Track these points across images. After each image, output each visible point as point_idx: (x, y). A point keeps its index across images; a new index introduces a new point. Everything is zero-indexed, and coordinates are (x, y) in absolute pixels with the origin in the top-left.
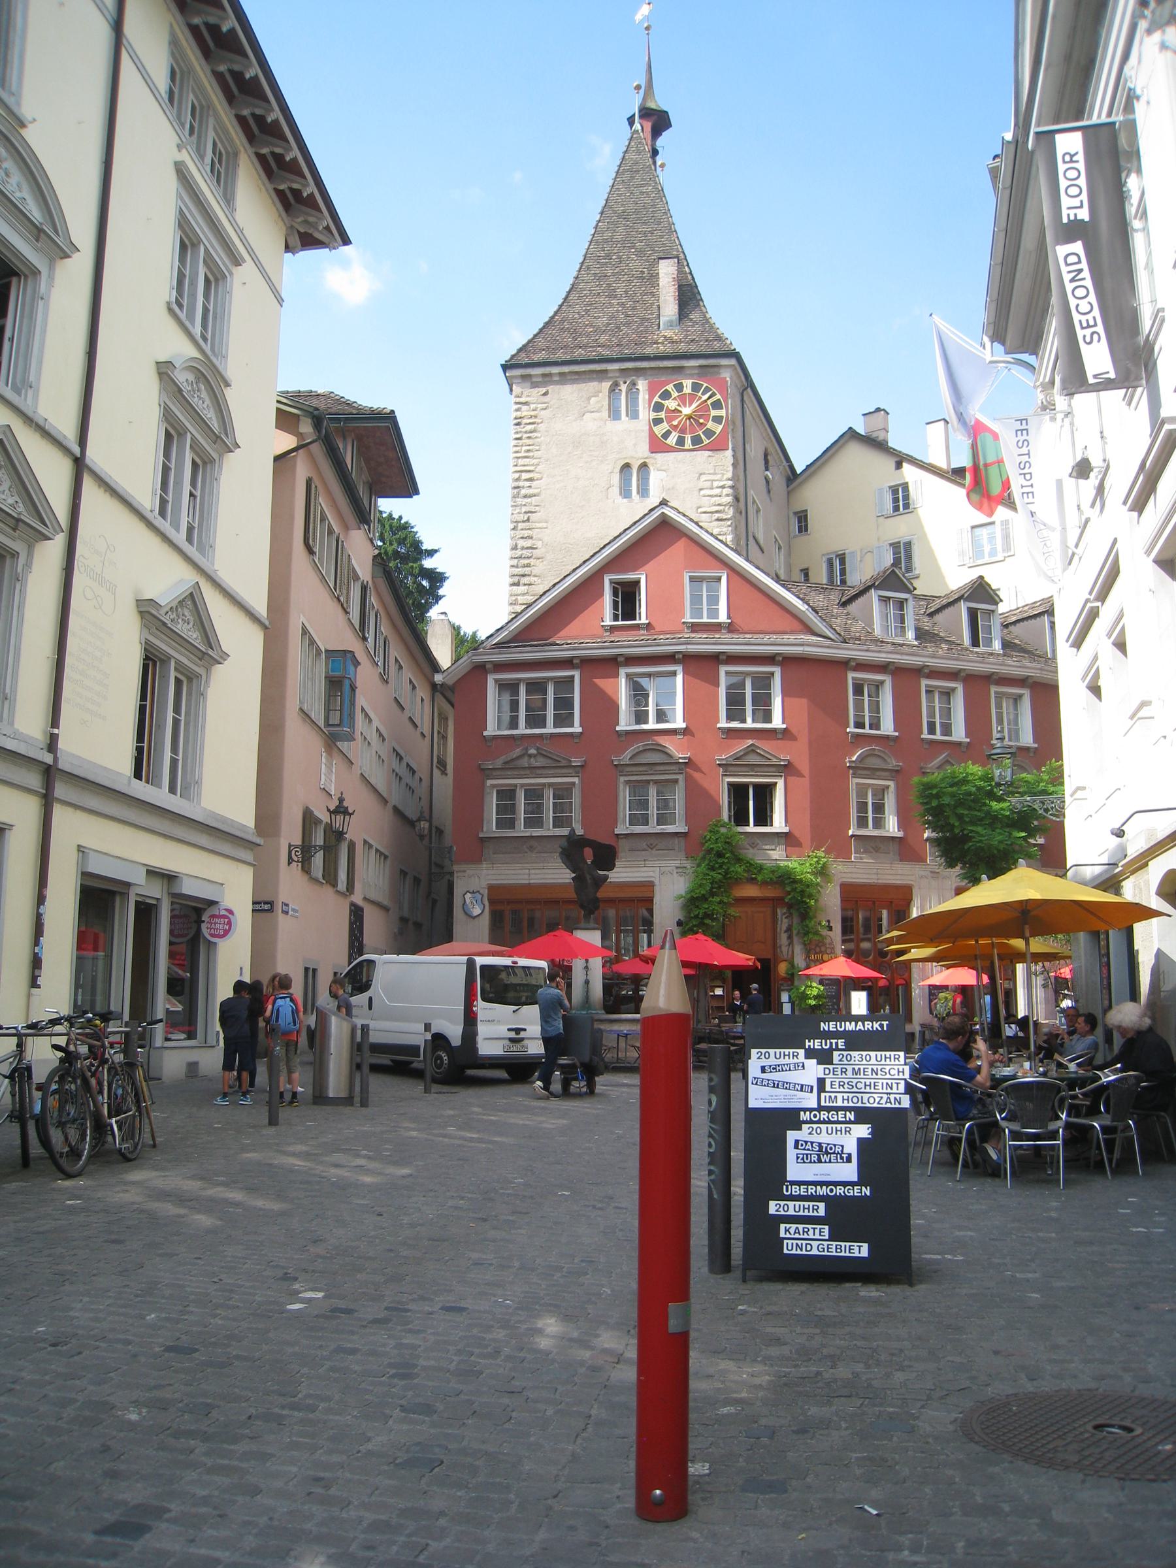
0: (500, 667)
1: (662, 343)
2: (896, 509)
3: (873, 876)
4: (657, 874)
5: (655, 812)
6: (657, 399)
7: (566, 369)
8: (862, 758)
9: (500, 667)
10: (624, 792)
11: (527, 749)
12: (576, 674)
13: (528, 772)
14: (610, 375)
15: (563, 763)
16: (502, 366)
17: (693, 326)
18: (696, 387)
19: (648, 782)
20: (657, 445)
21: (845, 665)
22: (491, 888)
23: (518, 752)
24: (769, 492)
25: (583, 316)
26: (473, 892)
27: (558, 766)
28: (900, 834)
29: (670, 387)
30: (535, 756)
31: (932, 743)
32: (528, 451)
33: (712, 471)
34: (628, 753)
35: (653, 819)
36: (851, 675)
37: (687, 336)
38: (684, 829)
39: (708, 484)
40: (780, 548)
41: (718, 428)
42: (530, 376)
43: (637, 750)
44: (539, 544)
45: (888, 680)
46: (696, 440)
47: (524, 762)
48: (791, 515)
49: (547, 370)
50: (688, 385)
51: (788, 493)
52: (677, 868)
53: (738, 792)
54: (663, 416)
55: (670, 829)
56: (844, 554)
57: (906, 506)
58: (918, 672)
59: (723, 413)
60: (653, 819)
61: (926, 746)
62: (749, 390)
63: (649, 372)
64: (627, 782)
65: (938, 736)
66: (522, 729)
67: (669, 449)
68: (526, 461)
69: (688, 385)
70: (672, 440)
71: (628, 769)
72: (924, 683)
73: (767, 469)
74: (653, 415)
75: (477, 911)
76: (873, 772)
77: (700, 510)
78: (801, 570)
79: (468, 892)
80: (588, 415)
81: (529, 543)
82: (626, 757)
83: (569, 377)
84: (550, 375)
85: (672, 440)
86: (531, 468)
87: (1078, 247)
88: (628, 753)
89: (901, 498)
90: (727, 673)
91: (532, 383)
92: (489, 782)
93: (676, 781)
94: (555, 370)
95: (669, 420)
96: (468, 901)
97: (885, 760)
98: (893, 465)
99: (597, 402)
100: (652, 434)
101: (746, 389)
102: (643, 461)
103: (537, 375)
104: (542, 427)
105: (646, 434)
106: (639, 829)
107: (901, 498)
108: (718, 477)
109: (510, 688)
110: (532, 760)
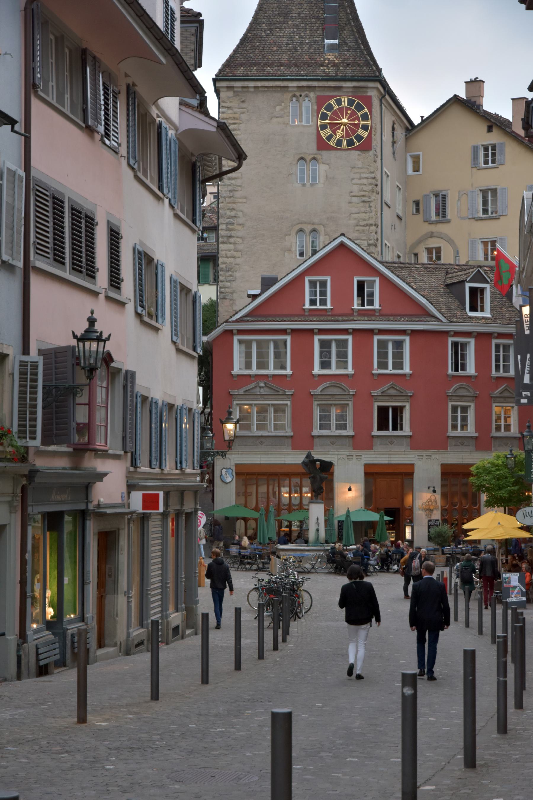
0: (241, 332)
1: (327, 66)
2: (486, 162)
3: (461, 460)
4: (336, 460)
5: (335, 422)
6: (323, 110)
7: (259, 84)
8: (455, 391)
9: (241, 332)
10: (317, 410)
11: (258, 383)
13: (259, 397)
14: (290, 89)
15: (281, 393)
17: (348, 51)
18: (351, 102)
19: (331, 405)
21: (446, 333)
22: (237, 465)
24: (394, 153)
26: (227, 469)
27: (277, 395)
28: (476, 435)
29: (332, 102)
30: (263, 387)
31: (498, 378)
35: (333, 427)
36: (450, 340)
37: (344, 60)
38: (352, 433)
39: (358, 176)
40: (400, 189)
41: (365, 134)
42: (233, 87)
44: (240, 214)
46: (350, 143)
47: (257, 391)
49: (246, 84)
52: (348, 456)
53: (383, 411)
55: (344, 433)
57: (493, 162)
58: (489, 335)
59: (369, 123)
60: (333, 427)
62: (387, 97)
63: (317, 89)
64: (318, 405)
65: (501, 373)
66: (254, 370)
67: (331, 148)
70: (332, 143)
71: (320, 397)
72: (494, 342)
74: (320, 122)
75: (229, 479)
76: (461, 398)
78: (414, 201)
79: (224, 468)
80: (275, 120)
81: (233, 213)
82: (318, 391)
83: (261, 89)
84: (248, 87)
85: (332, 143)
91: (234, 92)
93: (348, 405)
94: (251, 84)
96: (224, 473)
98: (485, 129)
99: (282, 110)
100: (318, 134)
101: (384, 97)
102: (313, 156)
104: (242, 126)
105: (314, 137)
106: (325, 432)
108: (365, 170)
109: (248, 344)
110: (262, 389)
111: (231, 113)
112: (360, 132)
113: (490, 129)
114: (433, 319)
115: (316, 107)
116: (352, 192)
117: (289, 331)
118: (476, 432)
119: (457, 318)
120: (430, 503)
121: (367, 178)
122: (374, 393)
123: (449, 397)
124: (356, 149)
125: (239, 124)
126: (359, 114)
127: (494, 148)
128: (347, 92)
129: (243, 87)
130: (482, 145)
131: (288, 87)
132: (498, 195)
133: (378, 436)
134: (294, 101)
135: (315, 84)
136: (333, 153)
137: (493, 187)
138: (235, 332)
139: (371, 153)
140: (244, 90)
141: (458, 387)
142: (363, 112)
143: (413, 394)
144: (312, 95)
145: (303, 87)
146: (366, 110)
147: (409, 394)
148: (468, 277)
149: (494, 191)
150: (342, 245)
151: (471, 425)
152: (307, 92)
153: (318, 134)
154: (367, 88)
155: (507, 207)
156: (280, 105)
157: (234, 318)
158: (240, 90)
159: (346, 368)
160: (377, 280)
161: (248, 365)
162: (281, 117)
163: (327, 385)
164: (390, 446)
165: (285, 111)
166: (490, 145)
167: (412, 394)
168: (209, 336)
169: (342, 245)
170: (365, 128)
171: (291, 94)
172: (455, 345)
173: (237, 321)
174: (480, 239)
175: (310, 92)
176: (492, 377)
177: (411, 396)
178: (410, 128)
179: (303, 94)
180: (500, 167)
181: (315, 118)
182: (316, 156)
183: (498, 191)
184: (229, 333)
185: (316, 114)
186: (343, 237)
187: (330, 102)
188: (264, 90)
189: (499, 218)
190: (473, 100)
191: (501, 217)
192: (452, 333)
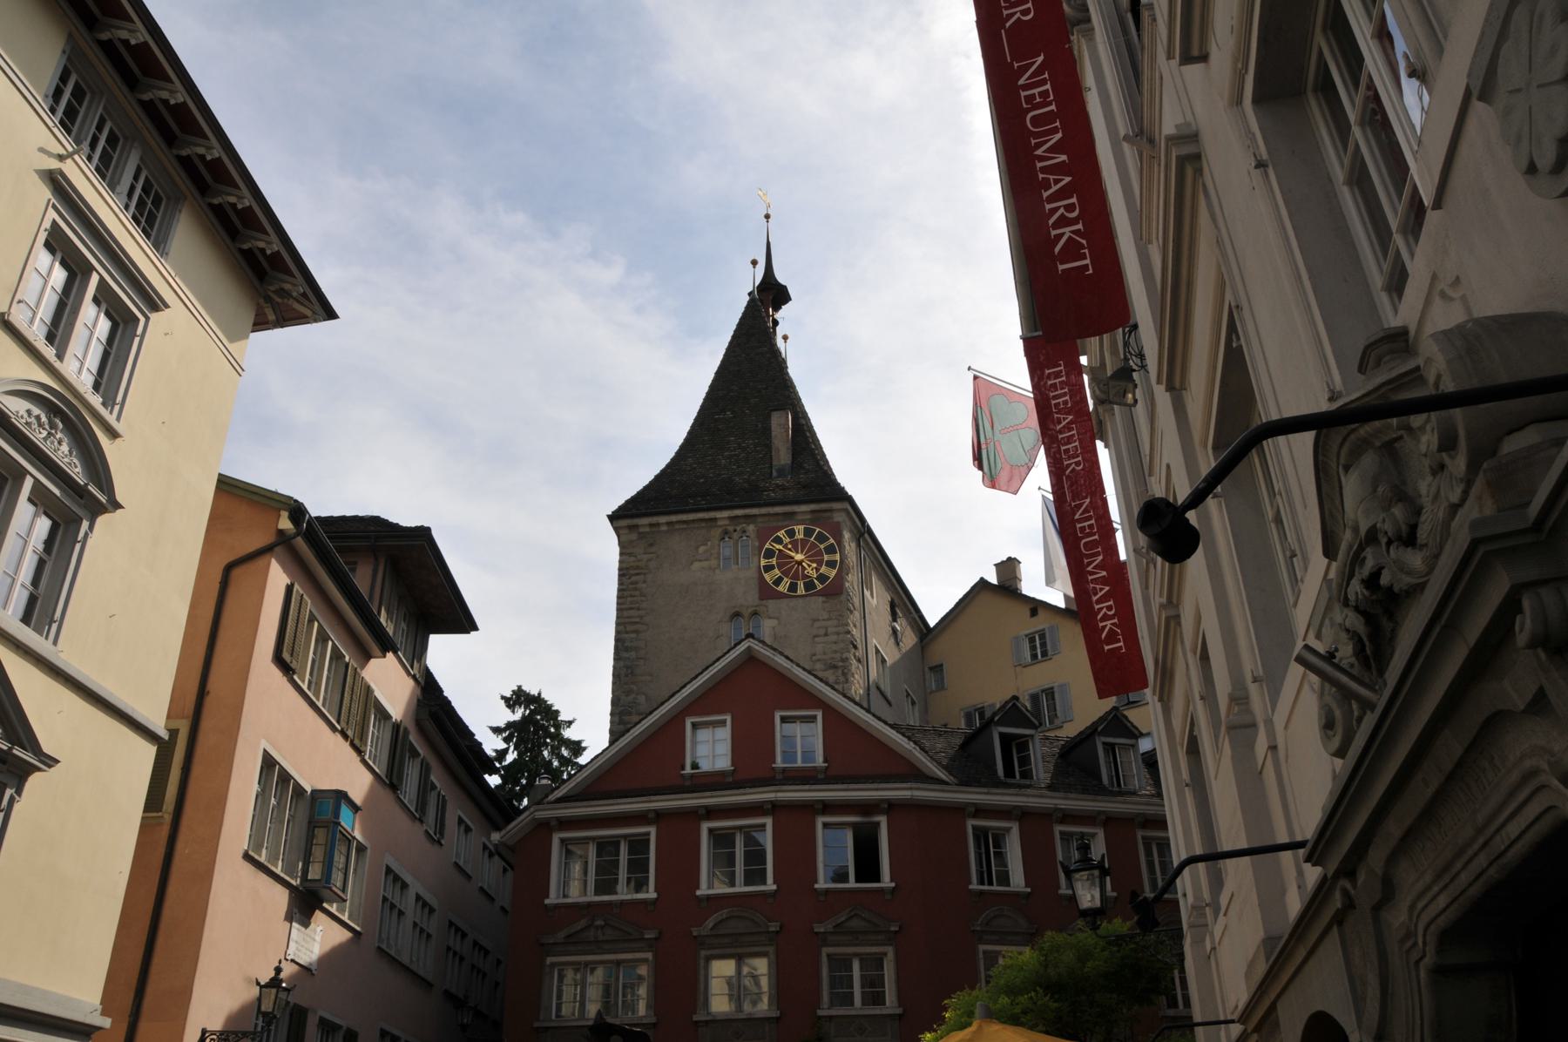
1: (773, 491)
2: (1034, 656)
7: (674, 518)
12: (652, 830)
14: (720, 523)
16: (609, 516)
18: (808, 532)
20: (767, 592)
21: (960, 810)
23: (583, 923)
25: (695, 468)
32: (631, 603)
33: (826, 617)
34: (710, 923)
36: (971, 823)
39: (822, 632)
40: (913, 703)
41: (832, 573)
42: (636, 526)
43: (720, 918)
44: (642, 699)
46: (809, 586)
48: (926, 669)
49: (654, 520)
50: (800, 531)
51: (923, 648)
54: (774, 563)
56: (983, 707)
57: (1044, 654)
59: (837, 557)
62: (866, 535)
63: (760, 520)
68: (632, 613)
69: (800, 531)
70: (783, 588)
73: (895, 620)
74: (763, 562)
77: (814, 658)
80: (696, 565)
83: (677, 526)
84: (658, 525)
85: (783, 588)
86: (637, 620)
88: (710, 923)
89: (1038, 645)
90: (826, 825)
92: (549, 960)
94: (663, 519)
95: (780, 566)
98: (1028, 613)
101: (862, 535)
102: (754, 609)
103: (644, 526)
107: (1038, 645)
111: (634, 562)
112: (823, 569)
113: (1034, 612)
115: (757, 544)
116: (814, 655)
117: (651, 815)
121: (838, 634)
122: (819, 928)
124: (820, 593)
125: (645, 574)
126: (822, 546)
127: (1042, 636)
128: (803, 520)
129: (651, 525)
130: (1026, 636)
131: (715, 520)
132: (1056, 696)
133: (831, 1017)
134: (727, 539)
135: (755, 511)
136: (785, 601)
138: (553, 823)
139: (843, 597)
140: (654, 529)
142: (826, 544)
144: (751, 528)
145: (737, 517)
146: (832, 541)
147: (893, 929)
149: (1050, 693)
150: (750, 659)
152: (744, 525)
153: (762, 579)
154: (831, 510)
156: (706, 544)
157: (551, 797)
158: (647, 529)
159: (764, 883)
160: (819, 714)
161: (585, 892)
162: (706, 560)
163: (724, 916)
165: (712, 551)
166: (1036, 632)
167: (897, 929)
168: (503, 832)
169: (750, 659)
170: (831, 564)
171: (720, 530)
172: (980, 833)
173: (559, 800)
175: (748, 524)
177: (896, 932)
178: (925, 631)
179: (738, 529)
180: (1055, 657)
181: (756, 559)
182: (757, 608)
184: (544, 828)
185: (757, 552)
186: (751, 640)
187: (778, 534)
188: (682, 527)
189: (1062, 727)
190: (1008, 584)
191: (1065, 725)
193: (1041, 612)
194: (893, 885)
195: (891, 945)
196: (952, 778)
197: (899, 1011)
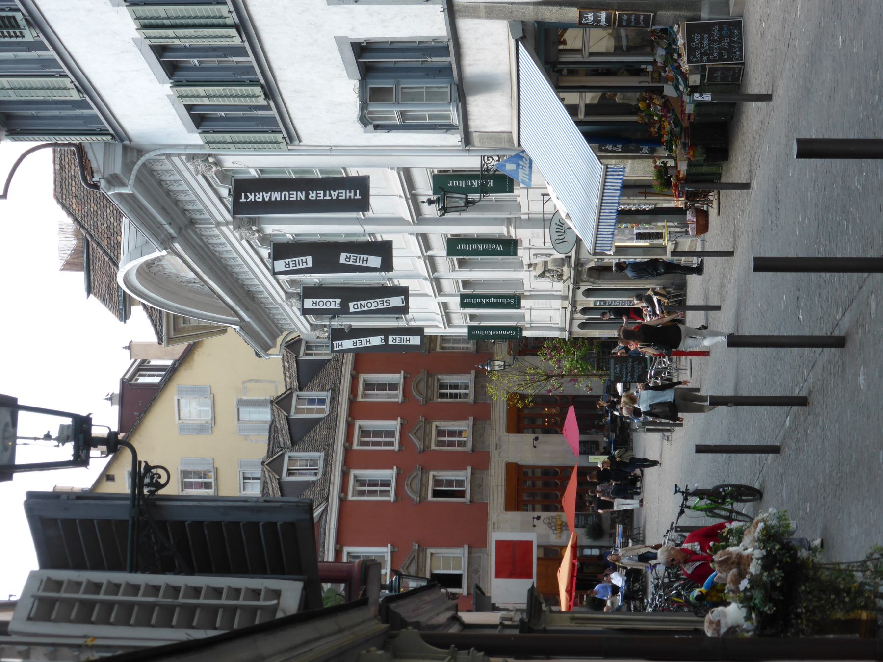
3: (500, 488)
21: (343, 501)
45: (353, 472)
61: (404, 448)
72: (355, 447)
87: (351, 304)
97: (414, 477)
114: (324, 517)
118: (467, 469)
119: (324, 490)
120: (553, 524)
123: (423, 499)
137: (179, 476)
141: (410, 490)
143: (416, 543)
147: (417, 548)
148: (275, 478)
151: (458, 476)
155: (203, 458)
164: (481, 572)
167: (417, 545)
174: (240, 492)
176: (399, 450)
177: (419, 546)
183: (184, 469)
189: (217, 468)
191: (215, 466)
192: (343, 495)
193: (111, 472)
194: (389, 545)
195: (426, 550)
196: (322, 504)
197: (466, 547)
